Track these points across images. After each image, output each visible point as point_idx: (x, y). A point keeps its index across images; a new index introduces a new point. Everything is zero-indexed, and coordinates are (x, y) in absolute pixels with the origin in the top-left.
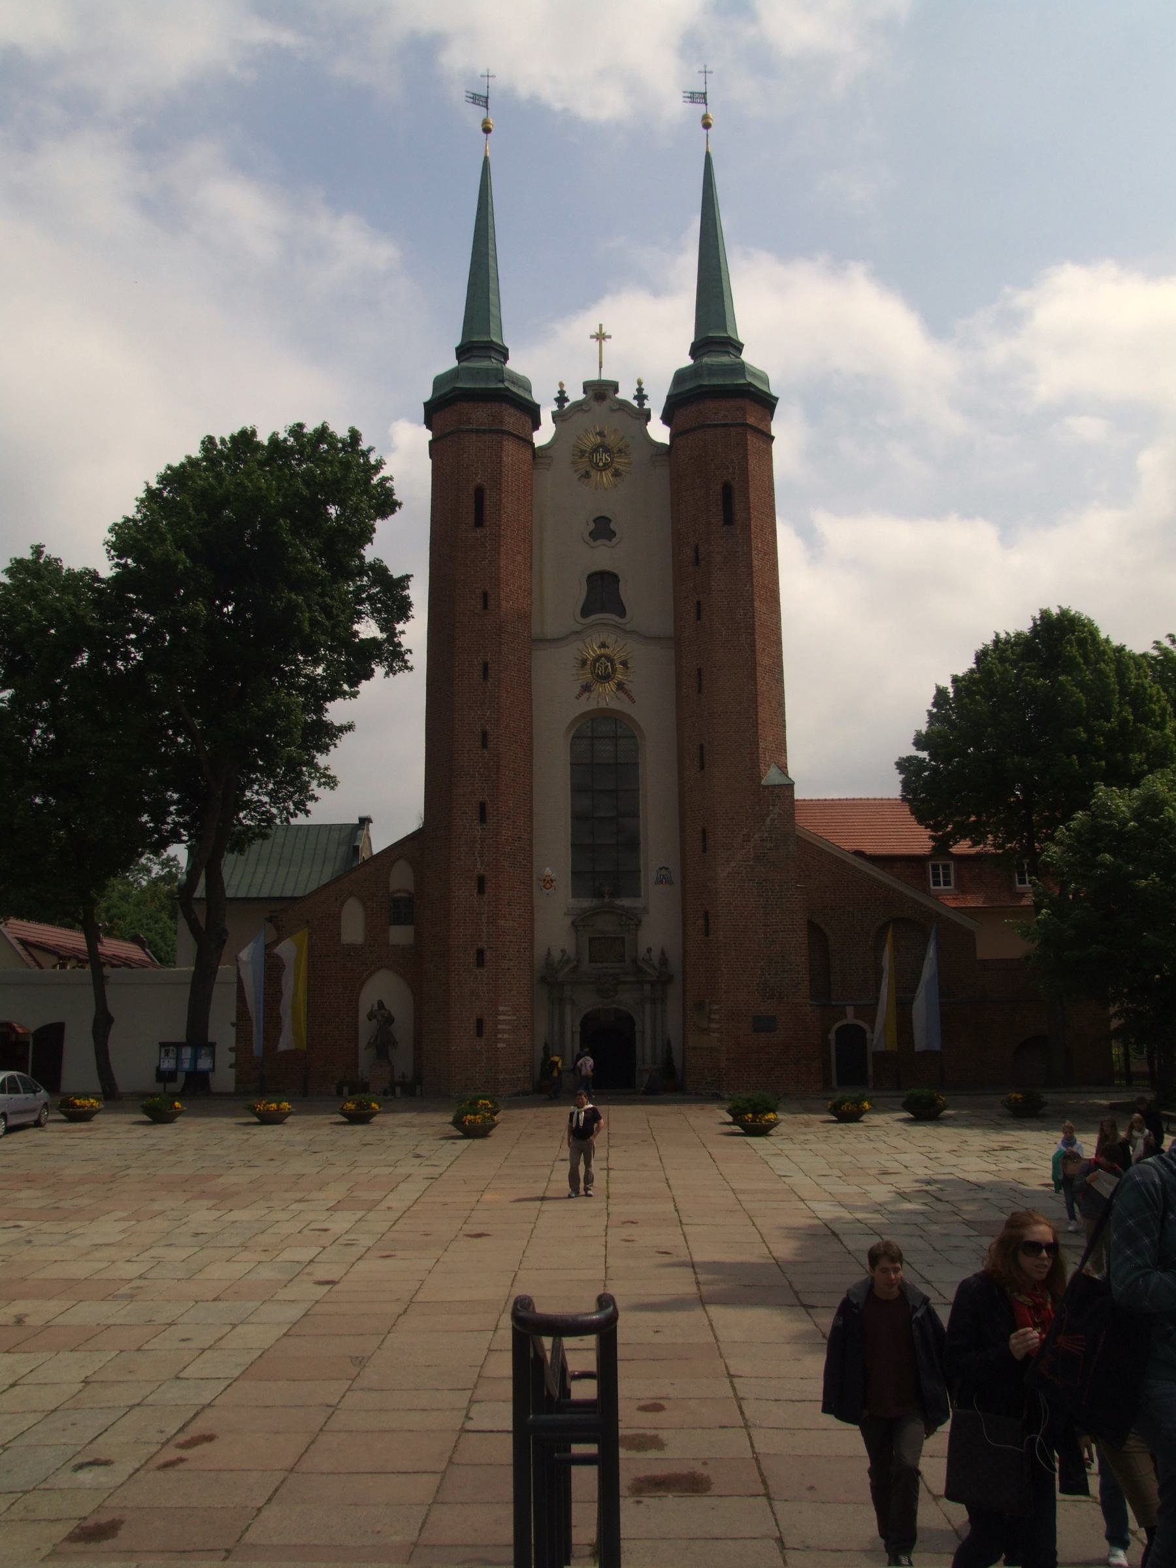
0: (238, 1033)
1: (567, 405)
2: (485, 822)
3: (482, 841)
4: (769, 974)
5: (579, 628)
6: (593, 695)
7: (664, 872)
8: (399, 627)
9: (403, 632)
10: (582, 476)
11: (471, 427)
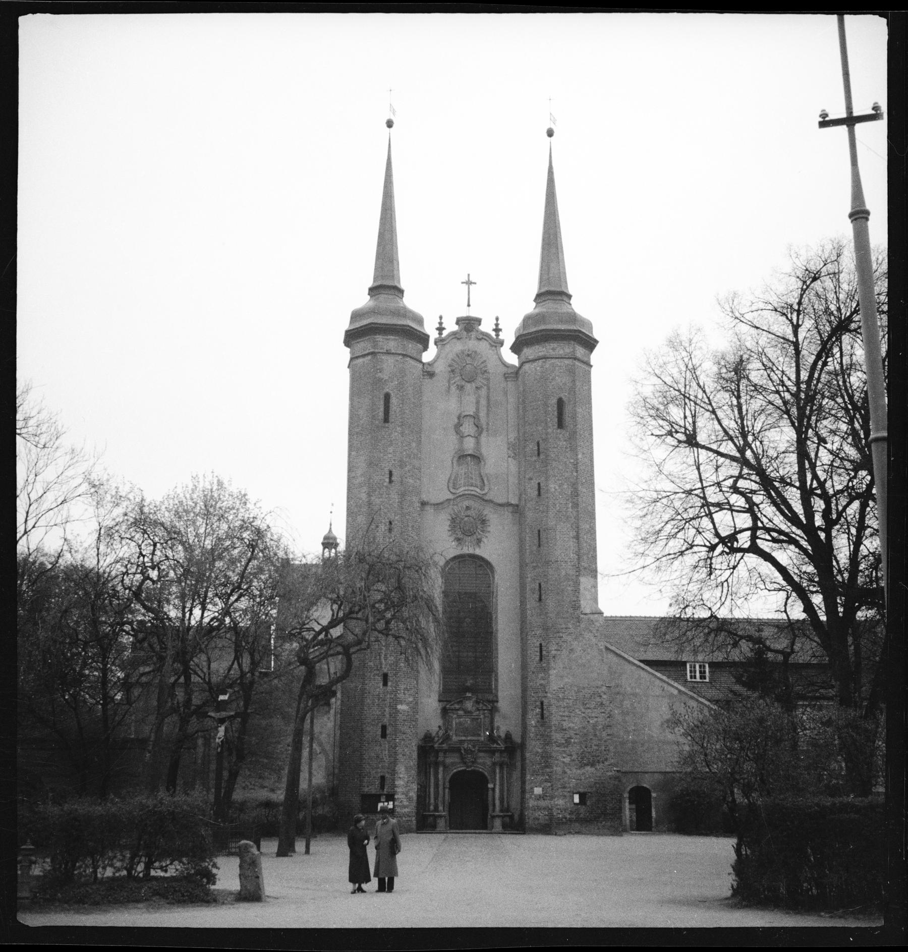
1: (445, 333)
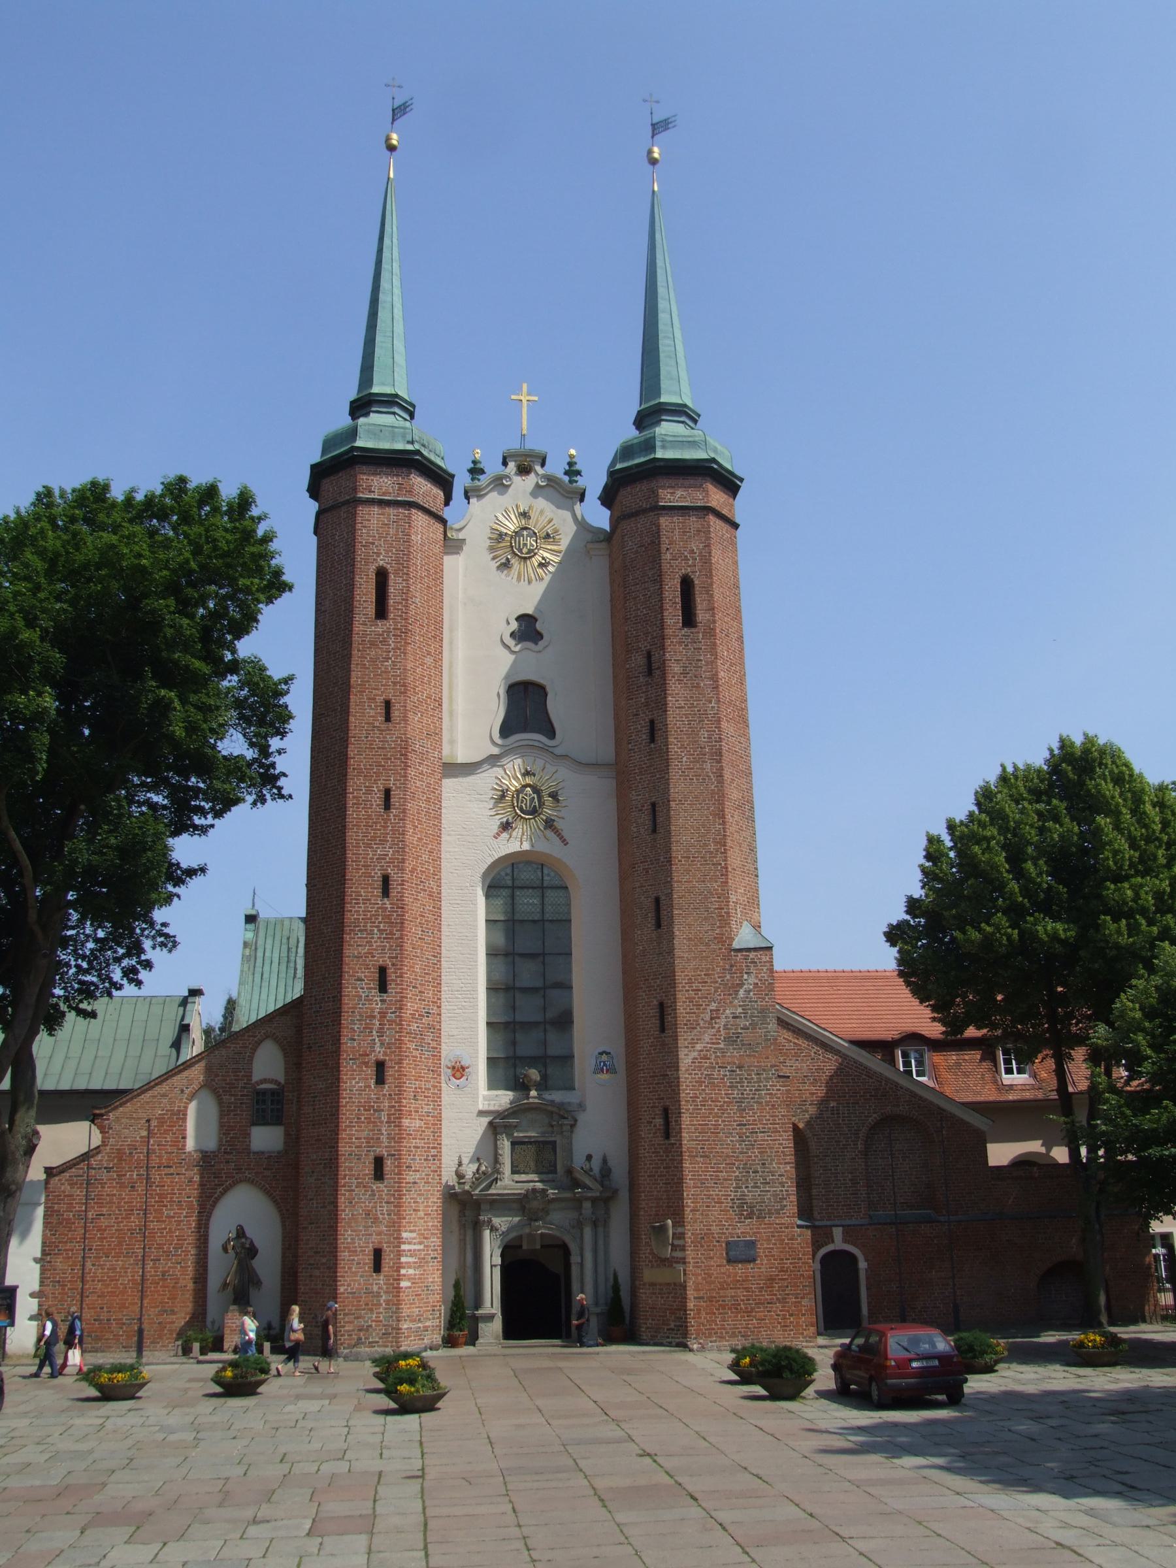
0: (43, 1271)
2: (386, 992)
3: (381, 1017)
4: (747, 1187)
5: (496, 751)
6: (514, 834)
7: (604, 1057)
8: (275, 743)
9: (280, 752)
10: (501, 564)
11: (372, 496)
